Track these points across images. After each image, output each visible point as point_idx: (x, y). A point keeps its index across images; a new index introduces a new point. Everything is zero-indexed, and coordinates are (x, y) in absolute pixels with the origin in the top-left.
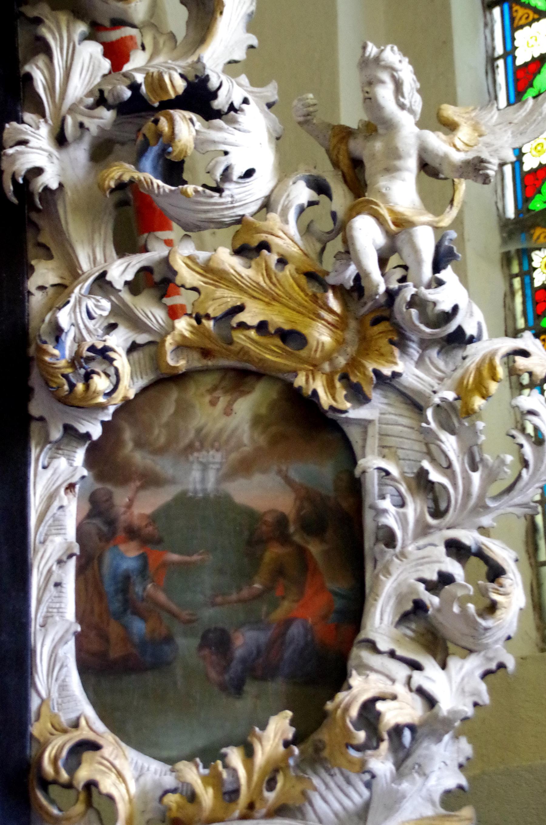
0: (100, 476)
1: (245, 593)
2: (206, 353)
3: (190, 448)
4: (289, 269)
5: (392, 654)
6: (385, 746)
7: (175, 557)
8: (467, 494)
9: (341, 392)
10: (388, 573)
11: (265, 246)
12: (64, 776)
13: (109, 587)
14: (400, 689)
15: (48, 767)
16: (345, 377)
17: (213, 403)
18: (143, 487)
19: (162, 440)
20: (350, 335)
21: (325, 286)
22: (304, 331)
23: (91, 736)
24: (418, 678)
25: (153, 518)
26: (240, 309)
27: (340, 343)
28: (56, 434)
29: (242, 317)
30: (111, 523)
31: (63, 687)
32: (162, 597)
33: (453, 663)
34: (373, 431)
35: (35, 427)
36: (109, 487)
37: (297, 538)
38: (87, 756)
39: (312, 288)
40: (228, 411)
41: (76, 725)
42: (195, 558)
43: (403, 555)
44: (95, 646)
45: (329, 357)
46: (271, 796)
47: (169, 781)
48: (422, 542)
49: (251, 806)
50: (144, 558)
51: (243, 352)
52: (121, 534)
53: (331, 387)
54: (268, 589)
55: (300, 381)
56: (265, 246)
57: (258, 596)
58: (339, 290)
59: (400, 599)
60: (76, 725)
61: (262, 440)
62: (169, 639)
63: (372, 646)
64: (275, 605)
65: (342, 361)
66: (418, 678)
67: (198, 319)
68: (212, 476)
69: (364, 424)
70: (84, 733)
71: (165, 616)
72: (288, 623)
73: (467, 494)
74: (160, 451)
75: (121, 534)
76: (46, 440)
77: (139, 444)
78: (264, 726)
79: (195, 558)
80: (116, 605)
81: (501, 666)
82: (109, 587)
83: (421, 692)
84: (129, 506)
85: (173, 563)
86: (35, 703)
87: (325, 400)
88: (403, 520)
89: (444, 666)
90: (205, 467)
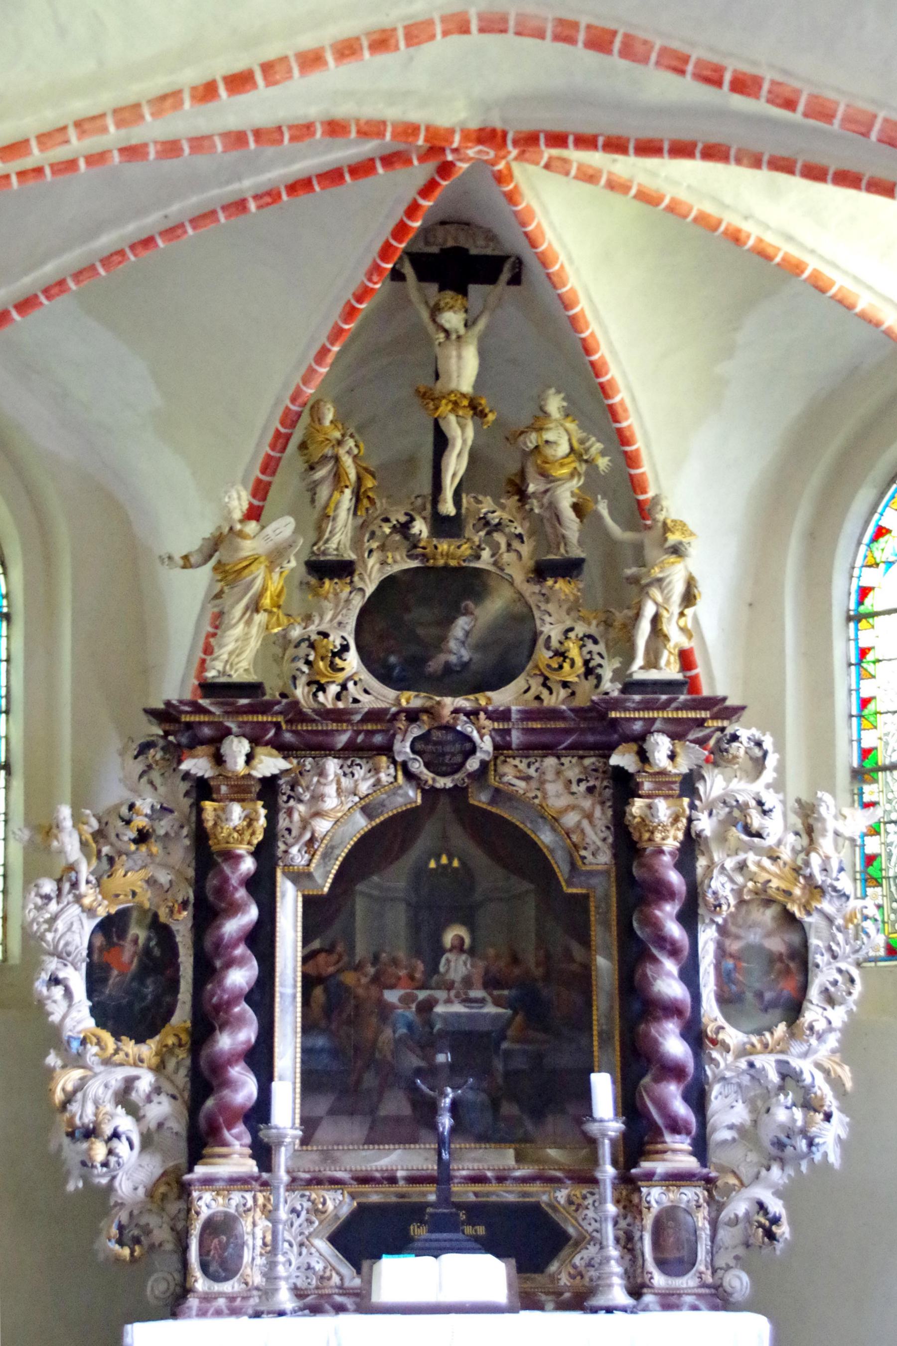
2: (757, 894)
3: (750, 927)
5: (817, 1005)
9: (803, 912)
11: (778, 858)
14: (819, 1017)
15: (709, 1033)
17: (758, 911)
21: (799, 874)
27: (803, 893)
28: (707, 921)
31: (711, 1007)
38: (721, 1031)
39: (795, 875)
40: (763, 913)
43: (822, 971)
45: (799, 899)
53: (800, 910)
58: (805, 877)
59: (821, 986)
60: (716, 1020)
62: (744, 993)
65: (803, 900)
69: (810, 924)
74: (740, 927)
76: (703, 922)
78: (777, 1026)
82: (724, 975)
87: (798, 914)
90: (755, 935)
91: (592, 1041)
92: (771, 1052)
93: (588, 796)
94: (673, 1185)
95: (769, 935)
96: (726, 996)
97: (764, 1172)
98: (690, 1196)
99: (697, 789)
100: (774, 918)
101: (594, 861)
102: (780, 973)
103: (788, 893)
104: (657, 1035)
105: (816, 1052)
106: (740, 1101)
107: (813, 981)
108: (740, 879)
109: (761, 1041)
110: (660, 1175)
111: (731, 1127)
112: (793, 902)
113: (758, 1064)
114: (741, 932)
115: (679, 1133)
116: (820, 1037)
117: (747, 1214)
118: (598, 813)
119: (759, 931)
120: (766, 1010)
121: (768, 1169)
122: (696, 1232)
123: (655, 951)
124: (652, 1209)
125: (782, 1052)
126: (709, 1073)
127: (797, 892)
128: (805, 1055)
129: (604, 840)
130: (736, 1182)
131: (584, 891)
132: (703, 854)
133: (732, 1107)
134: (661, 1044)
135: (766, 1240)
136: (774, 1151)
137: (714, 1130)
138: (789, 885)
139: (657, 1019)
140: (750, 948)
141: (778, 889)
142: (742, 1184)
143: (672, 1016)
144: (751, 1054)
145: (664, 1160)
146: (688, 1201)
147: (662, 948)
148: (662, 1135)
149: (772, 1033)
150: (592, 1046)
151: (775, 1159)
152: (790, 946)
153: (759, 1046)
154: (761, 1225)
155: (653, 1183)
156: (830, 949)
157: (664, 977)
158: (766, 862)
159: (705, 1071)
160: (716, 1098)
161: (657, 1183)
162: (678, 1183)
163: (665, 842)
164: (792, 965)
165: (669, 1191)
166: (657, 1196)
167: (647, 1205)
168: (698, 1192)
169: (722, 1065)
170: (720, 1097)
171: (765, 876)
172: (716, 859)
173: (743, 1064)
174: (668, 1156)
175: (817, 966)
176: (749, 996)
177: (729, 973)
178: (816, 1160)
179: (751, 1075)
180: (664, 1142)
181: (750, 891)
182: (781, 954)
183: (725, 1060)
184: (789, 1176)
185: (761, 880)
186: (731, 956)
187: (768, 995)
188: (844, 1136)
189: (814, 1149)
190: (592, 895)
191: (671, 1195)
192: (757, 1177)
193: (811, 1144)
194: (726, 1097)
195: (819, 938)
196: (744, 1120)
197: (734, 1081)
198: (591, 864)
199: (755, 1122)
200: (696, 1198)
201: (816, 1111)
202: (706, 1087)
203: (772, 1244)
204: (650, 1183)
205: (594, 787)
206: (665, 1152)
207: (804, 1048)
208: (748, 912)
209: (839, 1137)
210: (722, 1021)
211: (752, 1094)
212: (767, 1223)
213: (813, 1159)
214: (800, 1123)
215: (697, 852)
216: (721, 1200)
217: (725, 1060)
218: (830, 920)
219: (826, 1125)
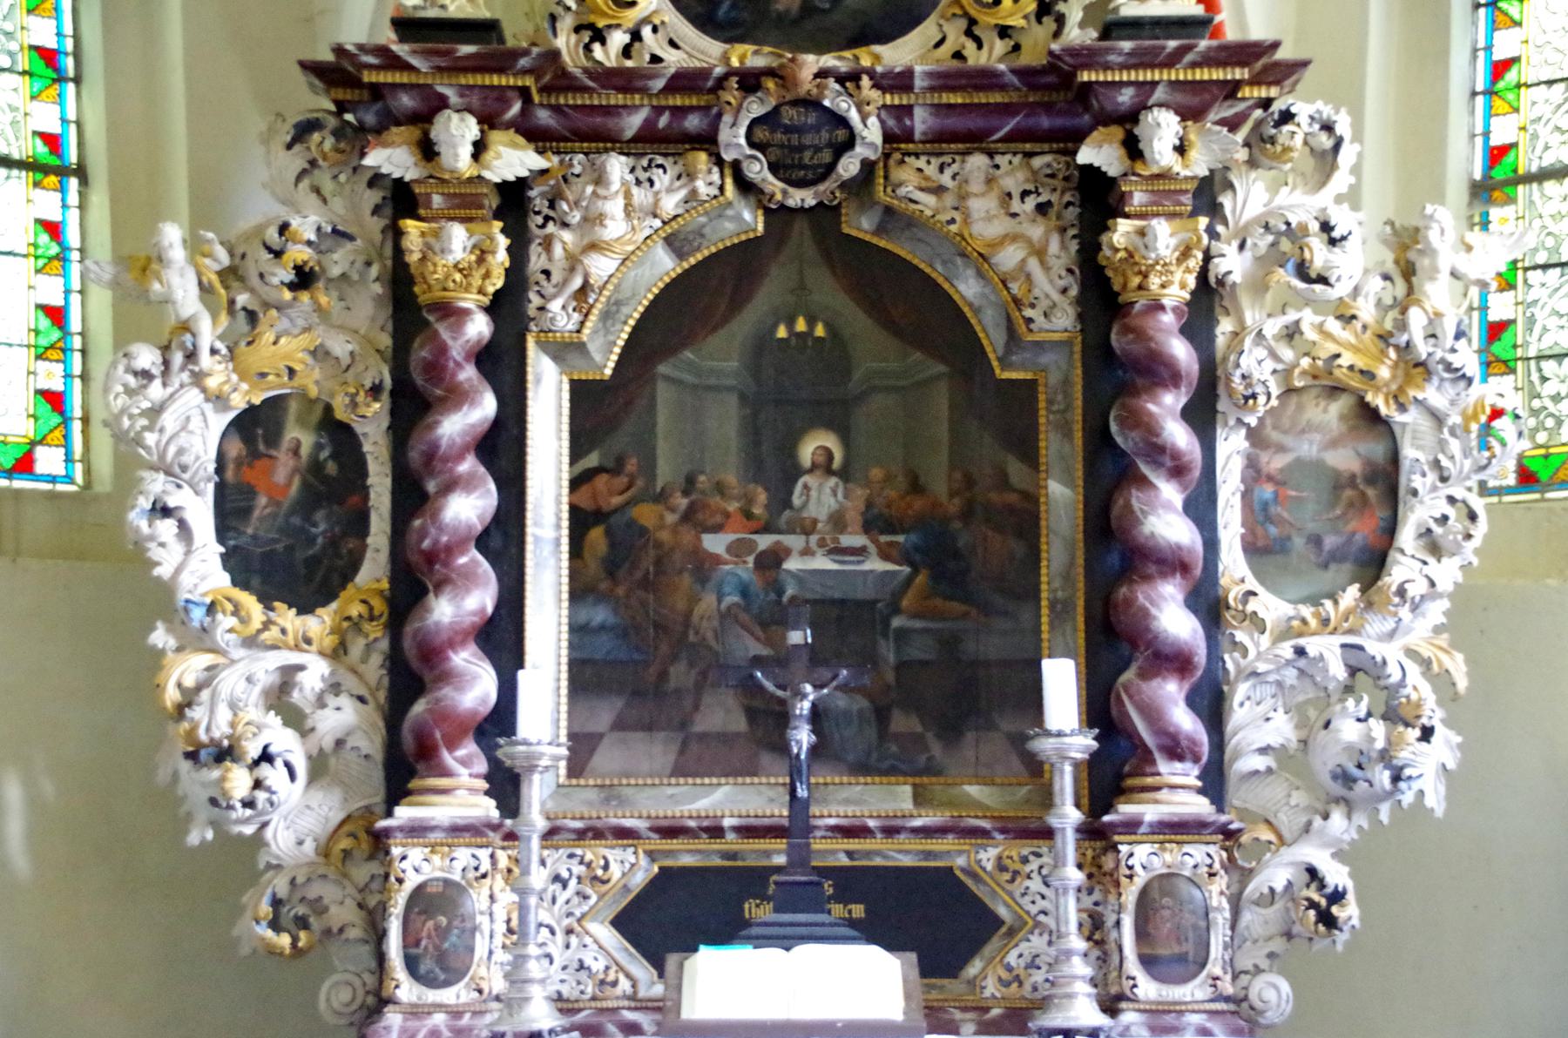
0: (1253, 445)
1: (1331, 516)
2: (1315, 377)
3: (1303, 431)
4: (1369, 333)
5: (1413, 557)
6: (1407, 605)
7: (1293, 493)
8: (1461, 472)
10: (1412, 511)
12: (1240, 607)
13: (1257, 507)
16: (1395, 397)
18: (1275, 453)
19: (1287, 426)
20: (1400, 372)
22: (1375, 371)
23: (1252, 588)
24: (1426, 570)
25: (1282, 470)
26: (1338, 356)
27: (1394, 377)
28: (1232, 422)
29: (1339, 361)
30: (1258, 471)
32: (1285, 515)
33: (1445, 560)
34: (1408, 429)
35: (1219, 417)
36: (1258, 451)
37: (1361, 487)
38: (1252, 598)
39: (1382, 345)
40: (1325, 411)
41: (1243, 581)
42: (1304, 494)
43: (1421, 502)
44: (1250, 539)
45: (1387, 385)
46: (1346, 625)
47: (1292, 613)
48: (1433, 495)
49: (1335, 629)
50: (1276, 494)
51: (1339, 380)
52: (1264, 478)
54: (1344, 514)
55: (1369, 398)
56: (1354, 317)
57: (1338, 518)
58: (1397, 347)
59: (1419, 526)
60: (1243, 581)
61: (1344, 428)
62: (1289, 538)
63: (1402, 551)
64: (1347, 523)
65: (1394, 387)
66: (1426, 570)
67: (1314, 359)
68: (1315, 448)
69: (1404, 425)
70: (1248, 586)
71: (1287, 526)
72: (1353, 533)
73: (1461, 472)
74: (1285, 432)
75: (1264, 478)
77: (1275, 427)
78: (1344, 591)
79: (1304, 494)
80: (1261, 519)
81: (1470, 563)
82: (1257, 507)
83: (1427, 576)
84: (1268, 463)
85: (1292, 497)
86: (1221, 568)
87: (1383, 411)
88: (1424, 485)
89: (1439, 561)
90: (1311, 443)
91: (1039, 616)
92: (1334, 632)
93: (1040, 219)
94: (1170, 842)
95: (1333, 444)
96: (1260, 544)
97: (1318, 822)
98: (1199, 860)
99: (1221, 205)
100: (1342, 417)
101: (1047, 326)
102: (1351, 505)
103: (1368, 375)
104: (1148, 605)
105: (1409, 631)
106: (1281, 710)
107: (1405, 517)
108: (1287, 354)
109: (1317, 615)
110: (1151, 825)
111: (1264, 751)
112: (1377, 389)
113: (1312, 651)
114: (1288, 440)
115: (1181, 758)
116: (1415, 608)
117: (1290, 884)
118: (1054, 246)
119: (1317, 437)
121: (1326, 817)
122: (1207, 914)
123: (1145, 469)
124: (1136, 879)
125: (1350, 631)
126: (1230, 665)
127: (1384, 372)
129: (1064, 291)
130: (1270, 836)
131: (1029, 376)
132: (1228, 314)
134: (1155, 618)
135: (1321, 928)
136: (1337, 789)
137: (1237, 755)
138: (1370, 362)
139: (1147, 578)
140: (1299, 463)
141: (1351, 368)
142: (1282, 841)
143: (1173, 573)
144: (1300, 635)
145: (1156, 802)
146: (1195, 867)
147: (1156, 464)
148: (1153, 762)
149: (1336, 602)
150: (1039, 625)
151: (1337, 800)
152: (1368, 462)
153: (1313, 623)
154: (1313, 905)
155: (1138, 838)
156: (1436, 464)
157: (1161, 511)
158: (1333, 325)
159: (1224, 662)
160: (1242, 704)
161: (1145, 838)
162: (1179, 838)
163: (1166, 291)
164: (1371, 493)
165: (1164, 850)
166: (1144, 861)
167: (1128, 872)
168: (1212, 853)
169: (1252, 654)
170: (1247, 704)
171: (1333, 348)
172: (1249, 321)
173: (1286, 650)
174: (1164, 794)
175: (1415, 493)
176: (1298, 542)
177: (1265, 506)
178: (1405, 804)
179: (1299, 669)
180: (1159, 774)
181: (1304, 373)
182: (1353, 477)
183: (1257, 645)
185: (1324, 355)
186: (1270, 478)
187: (1330, 542)
188: (1451, 765)
189: (1402, 785)
190: (1041, 381)
191: (1168, 857)
192: (1307, 829)
193: (1396, 779)
194: (1258, 704)
196: (1288, 740)
197: (1271, 678)
198: (1041, 330)
200: (1208, 861)
201: (1407, 725)
202: (1225, 688)
203: (1330, 935)
204: (1133, 838)
205: (1049, 203)
206: (1157, 788)
207: (1390, 624)
208: (1300, 408)
209: (1444, 766)
210: (1252, 583)
211: (1301, 698)
212: (1323, 902)
213: (1399, 801)
214: (1380, 744)
215: (1218, 310)
216: (1247, 865)
217: (1257, 645)
218: (1438, 418)
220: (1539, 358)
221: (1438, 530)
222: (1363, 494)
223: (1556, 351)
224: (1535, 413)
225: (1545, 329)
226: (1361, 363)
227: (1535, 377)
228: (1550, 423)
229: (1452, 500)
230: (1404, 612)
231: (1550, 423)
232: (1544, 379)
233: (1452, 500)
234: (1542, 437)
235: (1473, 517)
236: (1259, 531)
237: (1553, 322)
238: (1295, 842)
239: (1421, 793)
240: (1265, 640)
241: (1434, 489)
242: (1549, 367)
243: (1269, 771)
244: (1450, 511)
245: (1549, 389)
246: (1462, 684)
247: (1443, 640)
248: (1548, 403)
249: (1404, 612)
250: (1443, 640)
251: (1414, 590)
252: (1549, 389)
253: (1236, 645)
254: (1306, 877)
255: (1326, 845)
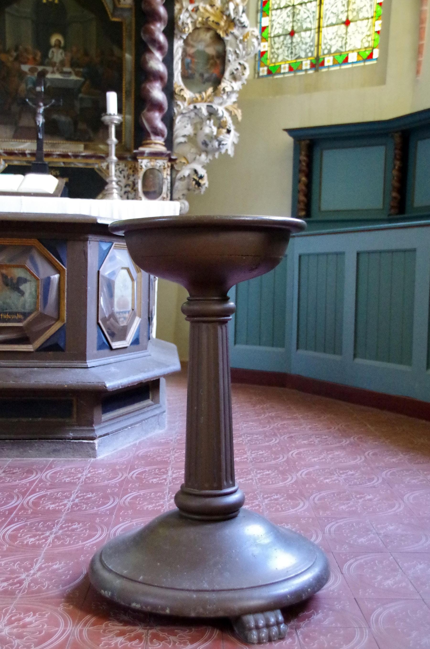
14: (229, 86)
27: (225, 25)
31: (179, 80)
40: (206, 35)
45: (223, 27)
58: (226, 16)
62: (194, 74)
69: (228, 41)
76: (177, 38)
92: (205, 102)
95: (208, 46)
100: (211, 38)
103: (218, 24)
105: (226, 102)
108: (195, 16)
109: (200, 96)
111: (184, 136)
112: (221, 29)
116: (228, 96)
120: (204, 83)
121: (200, 155)
125: (210, 102)
127: (222, 24)
128: (221, 104)
133: (185, 127)
136: (203, 147)
141: (213, 21)
142: (188, 163)
149: (206, 93)
154: (194, 180)
156: (235, 52)
160: (178, 122)
169: (182, 107)
171: (207, 15)
173: (191, 107)
176: (197, 76)
177: (188, 64)
181: (200, 23)
184: (210, 160)
186: (190, 56)
187: (206, 75)
193: (220, 144)
195: (231, 46)
197: (187, 115)
199: (195, 134)
207: (220, 101)
208: (199, 35)
214: (215, 133)
217: (184, 105)
218: (236, 38)
219: (227, 135)
220: (275, 36)
221: (235, 72)
222: (216, 62)
223: (279, 34)
224: (272, 53)
225: (276, 28)
226: (216, 20)
227: (273, 43)
228: (276, 56)
229: (240, 64)
230: (225, 97)
231: (276, 56)
232: (275, 43)
233: (240, 64)
234: (274, 60)
235: (245, 68)
236: (186, 72)
237: (278, 26)
238: (191, 163)
239: (227, 150)
240: (186, 104)
241: (235, 60)
242: (276, 39)
243: (185, 142)
244: (239, 67)
245: (276, 46)
246: (240, 118)
247: (236, 105)
248: (276, 50)
249: (225, 97)
250: (236, 105)
251: (227, 89)
252: (276, 46)
253: (178, 105)
254: (193, 172)
255: (200, 164)
